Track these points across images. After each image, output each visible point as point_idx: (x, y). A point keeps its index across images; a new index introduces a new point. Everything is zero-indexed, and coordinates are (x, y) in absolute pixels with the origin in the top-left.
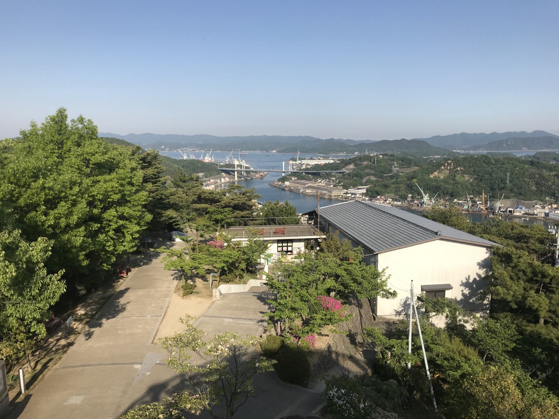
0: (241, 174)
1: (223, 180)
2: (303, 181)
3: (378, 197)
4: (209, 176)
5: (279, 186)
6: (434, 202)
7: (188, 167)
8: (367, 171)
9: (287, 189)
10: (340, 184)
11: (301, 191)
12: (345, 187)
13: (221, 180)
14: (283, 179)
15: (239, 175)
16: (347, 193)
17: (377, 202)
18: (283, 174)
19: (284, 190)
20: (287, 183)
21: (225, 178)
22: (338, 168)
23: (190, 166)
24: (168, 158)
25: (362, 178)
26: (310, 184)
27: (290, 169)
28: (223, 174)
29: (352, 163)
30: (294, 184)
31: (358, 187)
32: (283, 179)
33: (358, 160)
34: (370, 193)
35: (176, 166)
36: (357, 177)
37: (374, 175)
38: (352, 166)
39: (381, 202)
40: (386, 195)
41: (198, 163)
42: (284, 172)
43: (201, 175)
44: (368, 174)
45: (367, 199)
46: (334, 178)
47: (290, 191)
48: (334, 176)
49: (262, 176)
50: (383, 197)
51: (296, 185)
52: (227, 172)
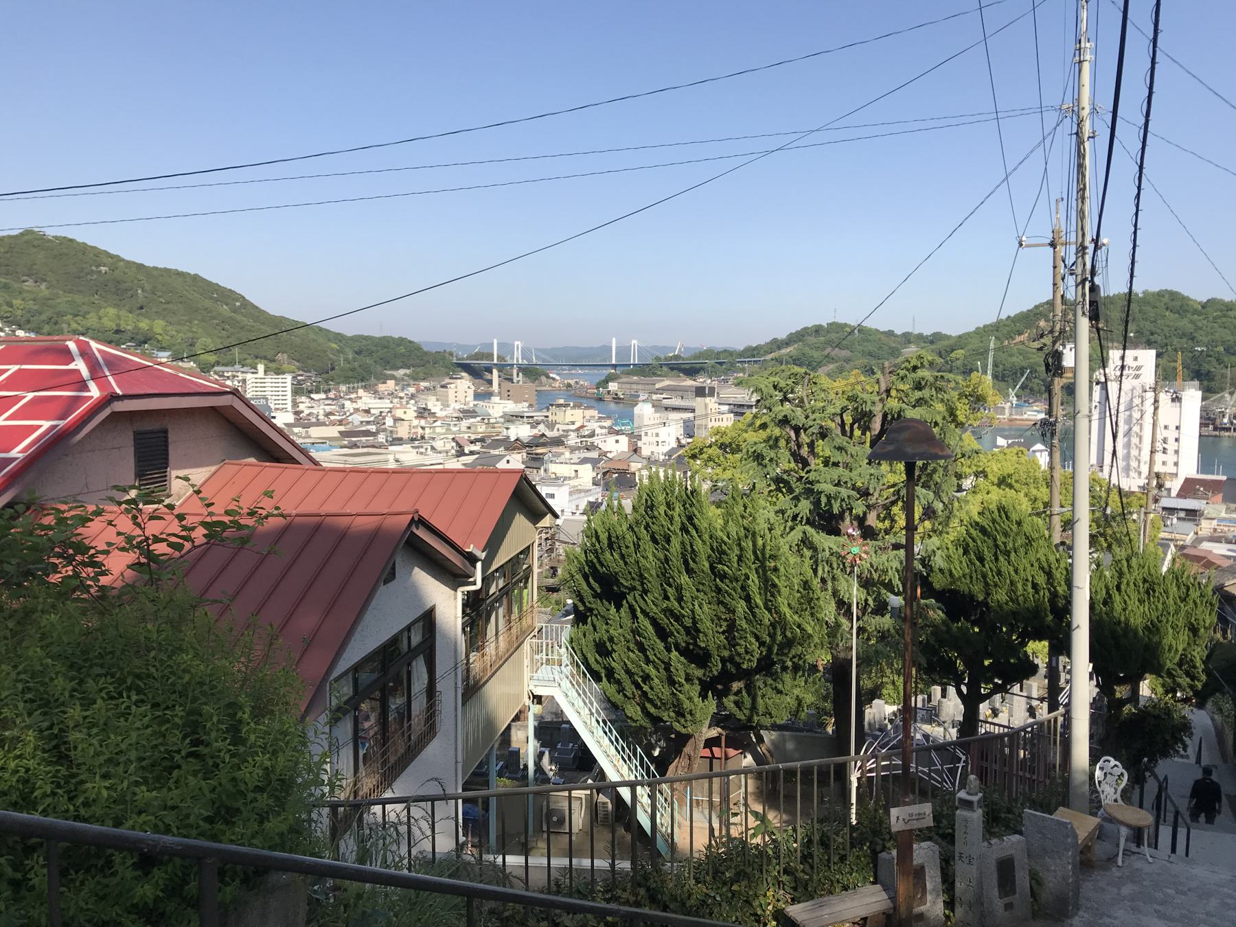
4: (421, 375)
6: (1014, 400)
9: (608, 398)
20: (613, 386)
22: (755, 353)
26: (667, 383)
28: (464, 374)
30: (628, 386)
33: (811, 335)
35: (334, 346)
41: (399, 345)
42: (615, 366)
47: (617, 399)
48: (743, 370)
49: (569, 385)
51: (634, 386)
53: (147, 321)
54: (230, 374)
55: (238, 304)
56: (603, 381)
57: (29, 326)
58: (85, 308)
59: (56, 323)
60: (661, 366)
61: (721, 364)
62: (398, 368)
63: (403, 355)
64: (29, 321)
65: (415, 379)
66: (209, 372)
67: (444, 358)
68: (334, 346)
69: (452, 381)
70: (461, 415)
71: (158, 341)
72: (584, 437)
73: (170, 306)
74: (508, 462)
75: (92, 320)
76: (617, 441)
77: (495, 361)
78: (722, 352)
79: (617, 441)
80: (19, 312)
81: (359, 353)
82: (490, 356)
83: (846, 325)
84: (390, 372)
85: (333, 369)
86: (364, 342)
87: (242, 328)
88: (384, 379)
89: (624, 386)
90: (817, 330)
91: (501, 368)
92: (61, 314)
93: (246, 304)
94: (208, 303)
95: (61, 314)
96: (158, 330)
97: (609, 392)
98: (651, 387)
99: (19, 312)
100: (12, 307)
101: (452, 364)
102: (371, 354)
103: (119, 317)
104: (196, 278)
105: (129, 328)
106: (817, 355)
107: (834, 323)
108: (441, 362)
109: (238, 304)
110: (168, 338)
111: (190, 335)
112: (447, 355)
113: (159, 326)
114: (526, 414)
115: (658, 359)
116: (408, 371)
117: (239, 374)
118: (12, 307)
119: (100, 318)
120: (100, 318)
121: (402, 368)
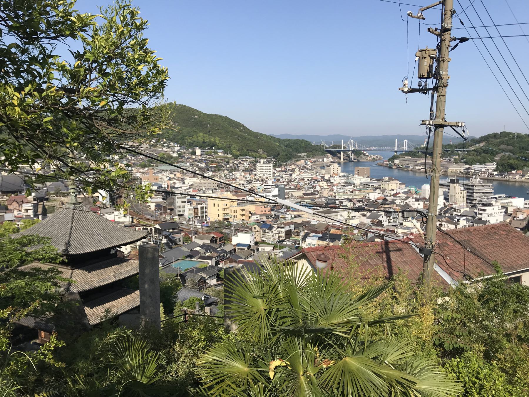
0: (349, 157)
1: (325, 160)
2: (416, 158)
3: (513, 172)
4: (311, 155)
5: (387, 165)
7: (291, 146)
8: (502, 147)
9: (394, 167)
10: (463, 161)
11: (411, 168)
12: (466, 163)
13: (323, 160)
14: (392, 159)
15: (347, 158)
16: (468, 169)
17: (511, 177)
18: (395, 154)
19: (391, 168)
20: (396, 161)
21: (328, 157)
23: (294, 146)
24: (272, 137)
25: (495, 156)
27: (405, 148)
28: (328, 155)
29: (484, 141)
30: (404, 162)
31: (487, 164)
32: (392, 159)
33: (492, 138)
34: (501, 169)
35: (277, 144)
36: (487, 153)
37: (511, 151)
38: (482, 145)
39: (517, 177)
40: (525, 168)
41: (302, 143)
42: (396, 152)
43: (303, 154)
44: (503, 150)
45: (495, 173)
46: (457, 157)
47: (399, 168)
48: (458, 155)
49: (374, 159)
50: (520, 171)
51: (407, 162)
52: (333, 154)
53: (213, 138)
54: (245, 159)
55: (242, 128)
56: (391, 158)
57: (174, 141)
58: (192, 133)
59: (183, 140)
60: (418, 151)
61: (447, 151)
62: (301, 153)
63: (304, 147)
64: (174, 139)
65: (309, 157)
66: (237, 158)
67: (320, 148)
68: (277, 144)
69: (332, 164)
70: (345, 185)
71: (218, 146)
72: (402, 200)
73: (219, 131)
74: (383, 217)
75: (195, 138)
76: (419, 204)
77: (342, 149)
78: (447, 145)
79: (419, 204)
80: (171, 136)
81: (286, 146)
82: (340, 147)
83: (510, 133)
84: (298, 154)
85: (279, 155)
86: (289, 142)
87: (245, 139)
88: (299, 158)
89: (402, 161)
90: (495, 136)
91: (344, 152)
92: (185, 136)
93: (245, 128)
94: (232, 129)
95: (185, 136)
96: (217, 142)
97: (395, 164)
98: (415, 163)
99: (171, 136)
100: (168, 133)
101: (324, 150)
102: (291, 146)
103: (204, 136)
104: (226, 118)
105: (208, 141)
106: (495, 149)
107: (503, 132)
108: (319, 150)
109: (242, 128)
110: (221, 144)
111: (228, 143)
112: (321, 146)
113: (217, 140)
114: (371, 184)
115: (417, 148)
116: (305, 154)
117: (248, 160)
118: (168, 133)
119: (198, 137)
120: (198, 137)
121: (303, 152)
